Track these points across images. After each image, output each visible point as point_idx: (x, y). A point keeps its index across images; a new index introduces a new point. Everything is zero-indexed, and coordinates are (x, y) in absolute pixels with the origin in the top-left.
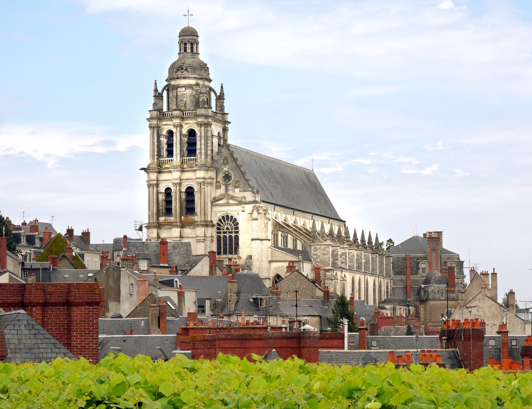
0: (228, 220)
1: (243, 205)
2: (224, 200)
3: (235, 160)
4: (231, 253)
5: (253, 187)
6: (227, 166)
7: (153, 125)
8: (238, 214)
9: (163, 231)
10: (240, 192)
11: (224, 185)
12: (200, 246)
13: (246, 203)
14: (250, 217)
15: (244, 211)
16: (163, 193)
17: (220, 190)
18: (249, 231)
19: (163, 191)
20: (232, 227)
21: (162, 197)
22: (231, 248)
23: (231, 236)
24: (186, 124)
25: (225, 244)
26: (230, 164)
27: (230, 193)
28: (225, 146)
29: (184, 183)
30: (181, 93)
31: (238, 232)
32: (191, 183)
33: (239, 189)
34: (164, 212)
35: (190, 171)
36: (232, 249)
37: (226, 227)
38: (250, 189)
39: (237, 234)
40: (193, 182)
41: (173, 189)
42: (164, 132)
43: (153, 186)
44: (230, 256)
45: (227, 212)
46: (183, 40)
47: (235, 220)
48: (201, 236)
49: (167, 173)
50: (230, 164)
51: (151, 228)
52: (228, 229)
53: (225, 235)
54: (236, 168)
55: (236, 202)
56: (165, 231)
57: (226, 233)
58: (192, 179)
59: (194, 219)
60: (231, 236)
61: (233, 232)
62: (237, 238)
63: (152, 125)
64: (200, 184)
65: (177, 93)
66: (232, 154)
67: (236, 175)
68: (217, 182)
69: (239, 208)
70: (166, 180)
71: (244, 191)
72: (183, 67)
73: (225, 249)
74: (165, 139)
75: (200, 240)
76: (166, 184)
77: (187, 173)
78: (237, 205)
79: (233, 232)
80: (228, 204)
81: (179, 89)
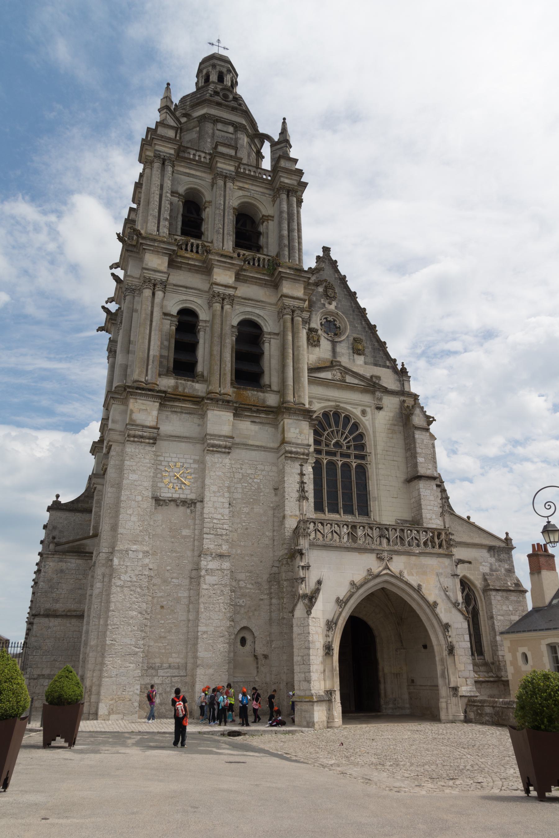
0: (337, 425)
1: (378, 394)
2: (334, 372)
3: (353, 296)
4: (349, 510)
5: (395, 360)
6: (334, 303)
7: (165, 154)
8: (364, 412)
9: (167, 417)
10: (366, 363)
11: (328, 339)
12: (293, 471)
13: (386, 391)
14: (395, 425)
15: (379, 408)
16: (172, 316)
17: (317, 349)
18: (395, 459)
19: (174, 312)
20: (348, 442)
21: (169, 326)
22: (348, 497)
23: (346, 466)
24: (241, 188)
25: (332, 484)
26: (340, 301)
27: (345, 360)
28: (327, 261)
29: (237, 307)
30: (223, 134)
31: (363, 457)
32: (257, 311)
33: (362, 358)
34: (171, 365)
35: (256, 284)
36: (351, 499)
37: (333, 442)
38: (388, 363)
39: (363, 462)
40: (263, 308)
41: (203, 315)
42: (181, 190)
43: (155, 285)
44: (349, 518)
45: (337, 404)
46: (217, 67)
47: (356, 426)
48: (299, 442)
49: (190, 270)
50: (340, 301)
51: (141, 395)
52: (337, 444)
53: (335, 458)
54: (354, 311)
55: (363, 384)
56: (174, 417)
57: (334, 454)
58: (262, 302)
59: (264, 401)
60: (346, 466)
61: (353, 457)
62: (362, 471)
63: (161, 154)
64: (293, 311)
65: (213, 130)
66: (343, 280)
67: (355, 327)
68: (311, 330)
69: (366, 399)
70: (186, 287)
71: (376, 365)
72: (229, 93)
73: (333, 496)
74: (181, 203)
75: (297, 453)
76: (184, 298)
77: (246, 285)
78: (364, 391)
79: (353, 457)
80: (343, 385)
81: (220, 126)
